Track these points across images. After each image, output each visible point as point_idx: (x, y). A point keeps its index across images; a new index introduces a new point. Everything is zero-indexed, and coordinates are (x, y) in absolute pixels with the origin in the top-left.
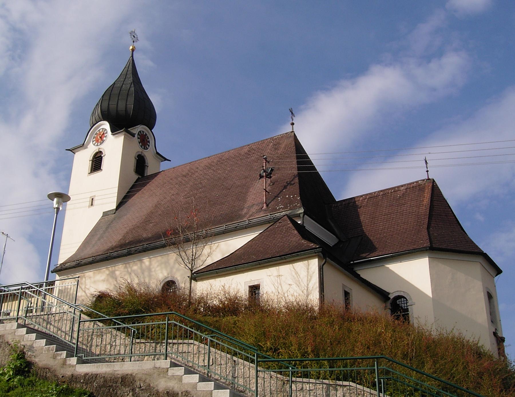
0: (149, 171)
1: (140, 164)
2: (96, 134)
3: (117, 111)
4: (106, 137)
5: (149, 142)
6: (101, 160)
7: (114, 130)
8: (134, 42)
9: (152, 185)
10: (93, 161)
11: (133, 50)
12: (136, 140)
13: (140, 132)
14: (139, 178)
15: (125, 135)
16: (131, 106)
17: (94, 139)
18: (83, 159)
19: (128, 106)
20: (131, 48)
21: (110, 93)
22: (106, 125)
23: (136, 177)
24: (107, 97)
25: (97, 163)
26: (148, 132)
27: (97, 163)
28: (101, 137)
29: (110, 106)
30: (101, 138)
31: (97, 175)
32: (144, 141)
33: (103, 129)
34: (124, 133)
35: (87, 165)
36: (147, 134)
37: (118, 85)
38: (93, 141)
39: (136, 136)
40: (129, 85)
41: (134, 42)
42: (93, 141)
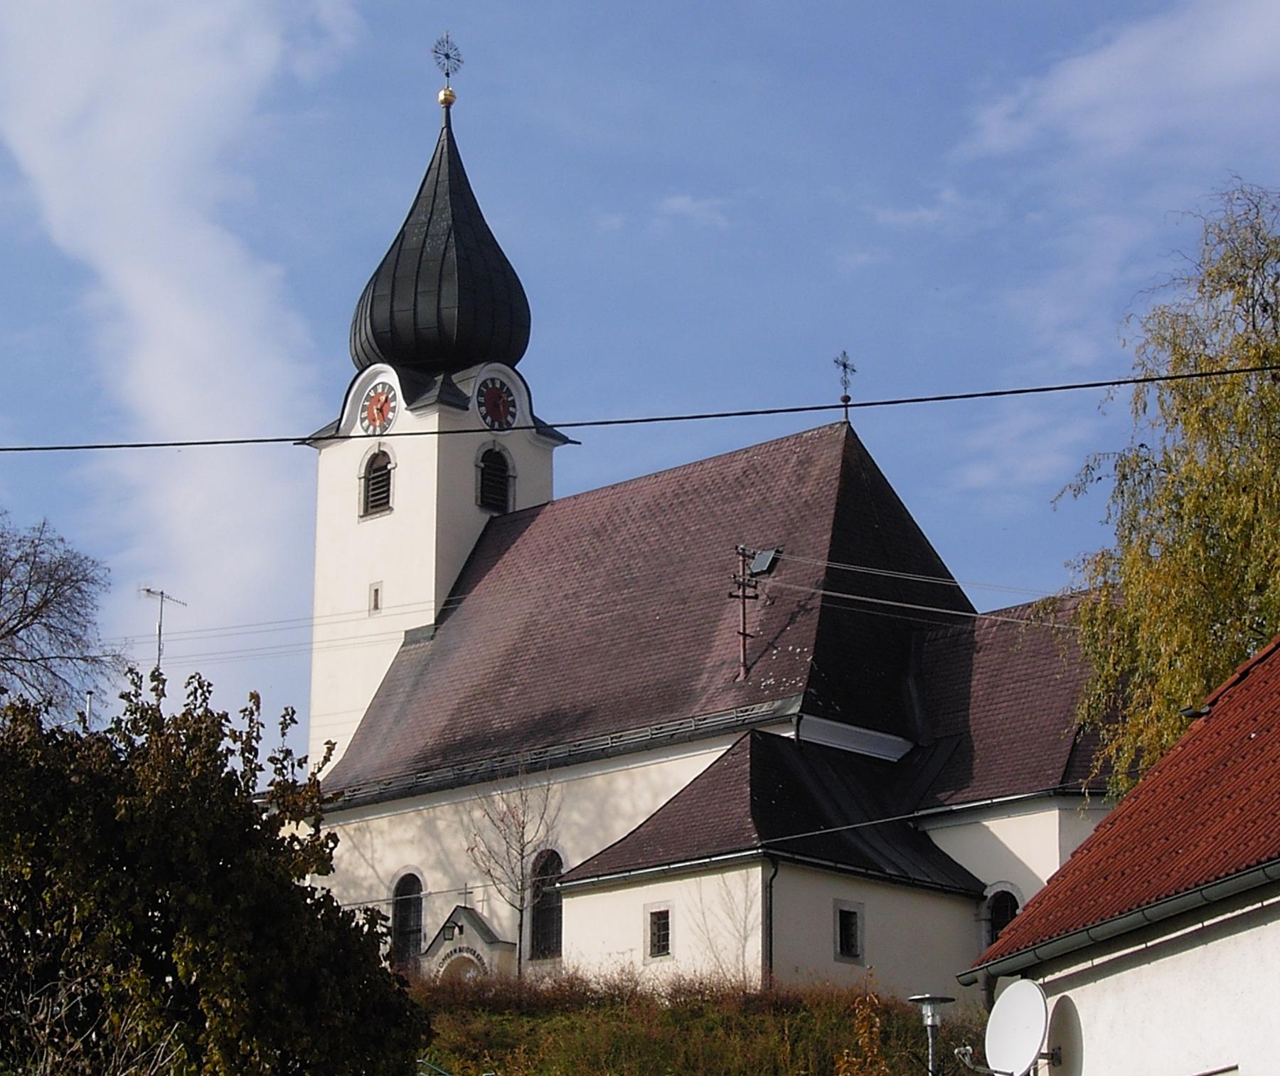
0: (521, 498)
1: (494, 476)
2: (368, 398)
3: (415, 324)
4: (393, 409)
5: (513, 404)
6: (389, 479)
7: (413, 395)
8: (447, 75)
9: (534, 537)
10: (367, 479)
11: (448, 103)
12: (474, 416)
13: (484, 384)
14: (492, 518)
15: (439, 411)
16: (451, 310)
17: (365, 415)
18: (343, 465)
19: (444, 312)
20: (442, 96)
21: (395, 272)
22: (388, 376)
23: (483, 518)
24: (385, 290)
25: (377, 487)
26: (509, 377)
27: (377, 487)
28: (381, 410)
29: (398, 316)
30: (380, 412)
31: (380, 522)
32: (498, 405)
33: (384, 384)
34: (436, 407)
35: (353, 491)
36: (505, 380)
37: (413, 241)
38: (362, 420)
39: (473, 404)
40: (444, 238)
41: (447, 75)
42: (362, 420)
